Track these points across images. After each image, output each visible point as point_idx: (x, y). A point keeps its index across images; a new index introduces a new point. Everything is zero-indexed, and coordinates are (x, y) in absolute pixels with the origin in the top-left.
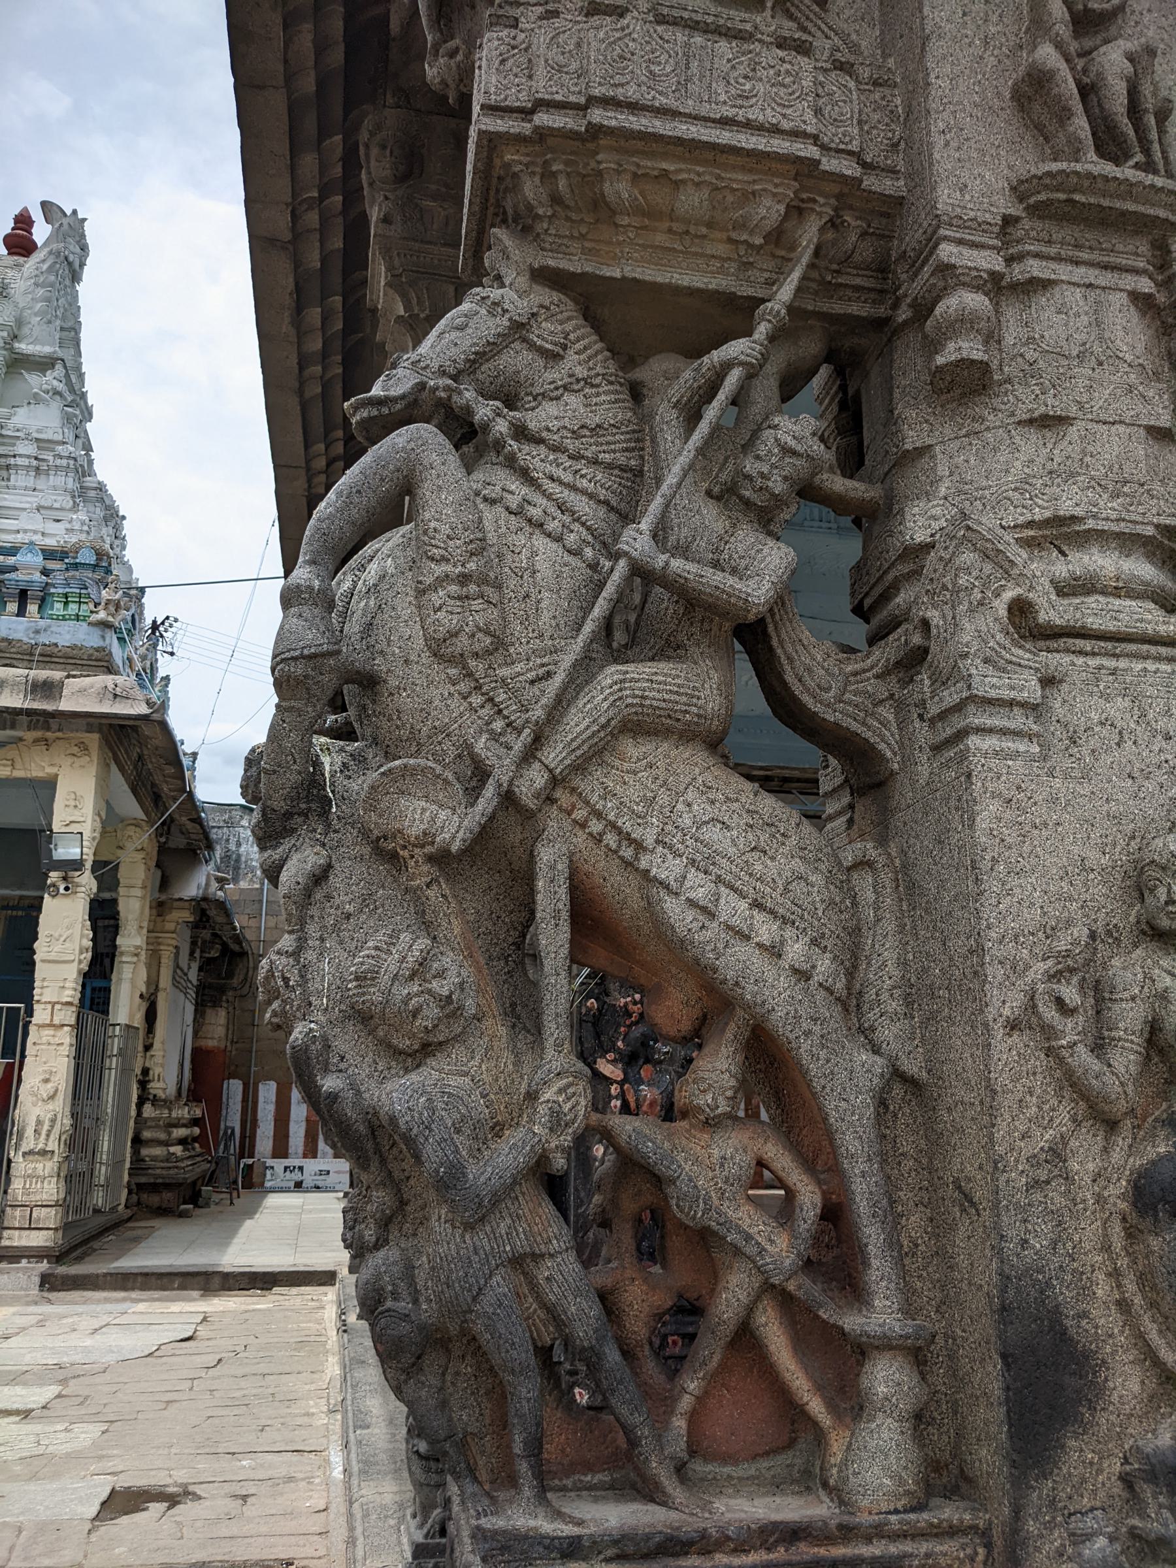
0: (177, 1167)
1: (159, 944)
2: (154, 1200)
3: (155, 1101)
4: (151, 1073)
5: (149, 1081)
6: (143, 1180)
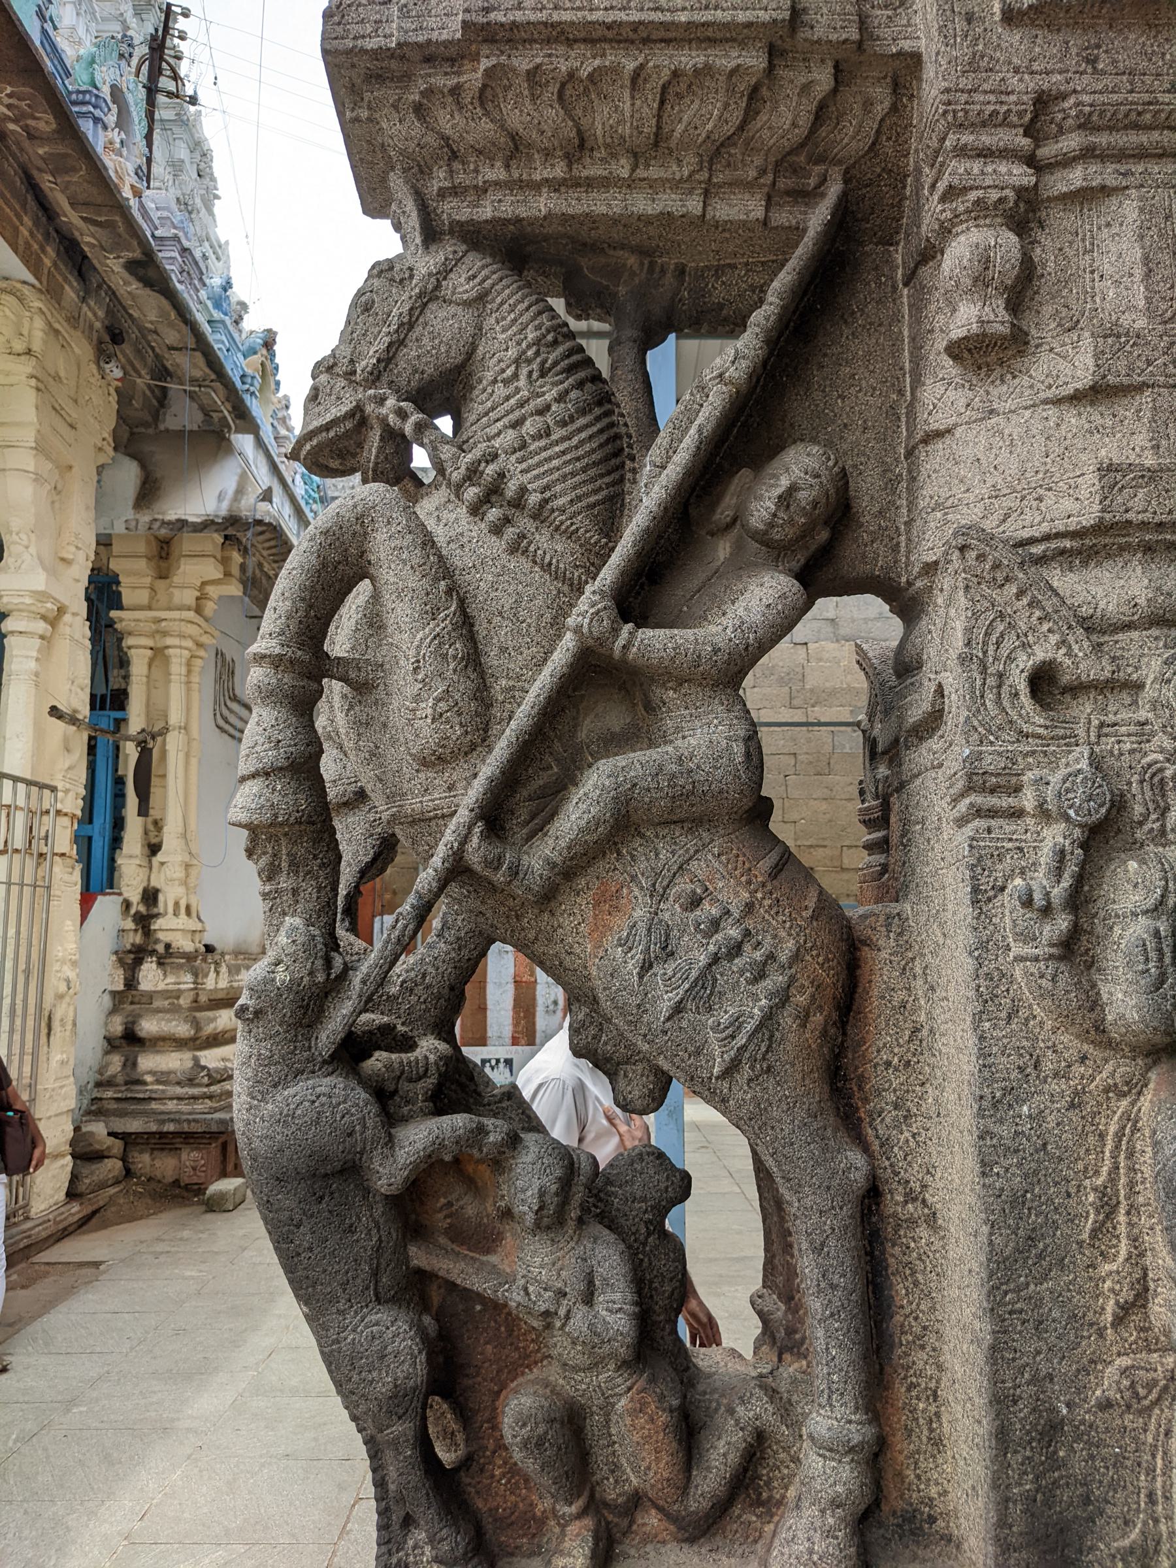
0: (210, 1097)
1: (165, 634)
2: (165, 1166)
3: (167, 957)
4: (161, 897)
5: (157, 916)
6: (134, 1125)
